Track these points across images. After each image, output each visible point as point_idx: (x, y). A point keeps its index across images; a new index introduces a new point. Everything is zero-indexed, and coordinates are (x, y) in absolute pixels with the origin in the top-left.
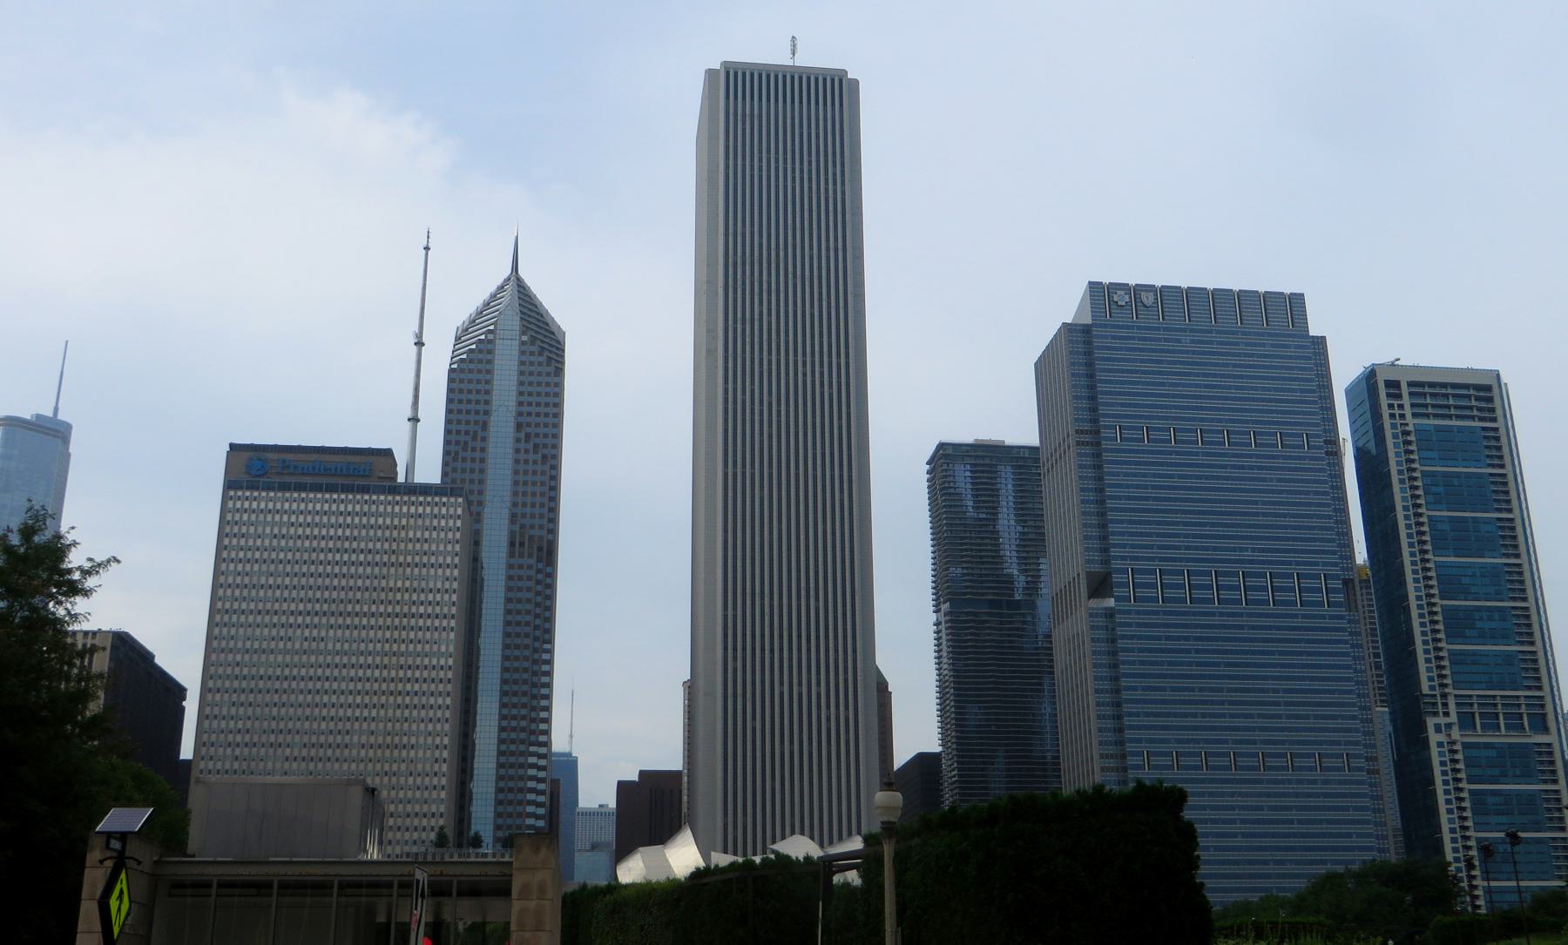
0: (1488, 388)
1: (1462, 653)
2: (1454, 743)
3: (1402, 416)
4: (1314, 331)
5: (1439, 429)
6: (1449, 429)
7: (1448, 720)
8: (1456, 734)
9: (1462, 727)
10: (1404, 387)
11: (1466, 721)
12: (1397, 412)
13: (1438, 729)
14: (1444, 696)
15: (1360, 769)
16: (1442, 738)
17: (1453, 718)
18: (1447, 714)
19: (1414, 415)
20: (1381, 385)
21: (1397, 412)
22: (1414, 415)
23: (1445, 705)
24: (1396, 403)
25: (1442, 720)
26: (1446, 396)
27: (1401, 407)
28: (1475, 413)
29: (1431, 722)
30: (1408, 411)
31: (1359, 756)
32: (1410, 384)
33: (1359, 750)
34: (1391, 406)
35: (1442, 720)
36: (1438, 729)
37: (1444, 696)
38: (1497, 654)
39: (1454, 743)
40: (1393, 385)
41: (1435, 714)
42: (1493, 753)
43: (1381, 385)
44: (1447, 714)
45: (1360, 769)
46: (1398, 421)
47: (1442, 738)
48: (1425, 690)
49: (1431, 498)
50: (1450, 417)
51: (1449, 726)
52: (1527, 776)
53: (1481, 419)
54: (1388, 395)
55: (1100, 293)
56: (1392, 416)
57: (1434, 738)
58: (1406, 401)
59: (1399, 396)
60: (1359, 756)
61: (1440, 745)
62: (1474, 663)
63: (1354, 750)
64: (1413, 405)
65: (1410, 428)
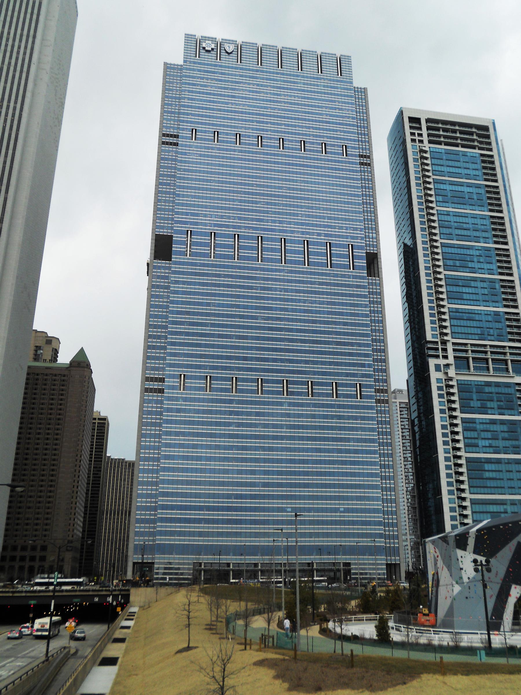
0: (486, 128)
2: (451, 379)
3: (421, 141)
4: (357, 83)
6: (457, 153)
7: (445, 362)
8: (452, 372)
9: (457, 368)
10: (423, 122)
11: (462, 363)
12: (417, 138)
14: (444, 342)
15: (370, 397)
17: (451, 360)
18: (446, 357)
19: (430, 142)
20: (406, 120)
21: (417, 138)
22: (430, 142)
23: (445, 350)
24: (416, 132)
25: (442, 362)
26: (454, 131)
27: (420, 135)
29: (432, 362)
30: (425, 138)
31: (370, 386)
32: (428, 121)
33: (370, 381)
34: (412, 134)
35: (442, 362)
36: (438, 368)
37: (444, 342)
39: (451, 379)
40: (415, 121)
41: (437, 357)
43: (406, 120)
44: (446, 357)
45: (370, 397)
46: (417, 144)
47: (440, 375)
48: (429, 338)
49: (440, 198)
50: (457, 145)
51: (447, 366)
53: (480, 149)
54: (411, 127)
56: (413, 140)
57: (434, 376)
58: (424, 132)
59: (420, 129)
60: (370, 386)
61: (438, 380)
63: (365, 381)
64: (429, 135)
65: (427, 149)
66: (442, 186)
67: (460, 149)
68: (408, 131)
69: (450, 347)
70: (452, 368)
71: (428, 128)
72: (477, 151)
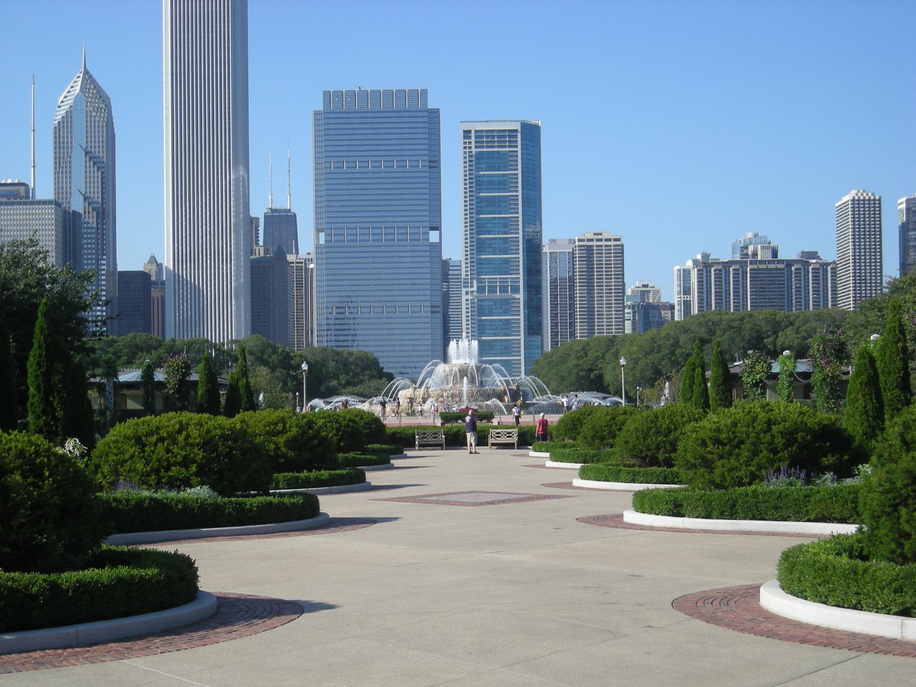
3: (470, 148)
5: (488, 152)
10: (473, 132)
11: (481, 289)
12: (467, 145)
13: (467, 293)
16: (469, 297)
17: (475, 289)
18: (472, 287)
19: (476, 147)
21: (467, 145)
22: (476, 147)
23: (472, 283)
25: (470, 289)
29: (464, 290)
30: (473, 145)
32: (476, 131)
35: (470, 289)
38: (500, 259)
42: (491, 303)
44: (472, 287)
47: (469, 297)
51: (472, 292)
52: (506, 312)
55: (327, 96)
57: (464, 297)
58: (473, 140)
61: (467, 300)
62: (491, 264)
67: (496, 149)
71: (476, 137)
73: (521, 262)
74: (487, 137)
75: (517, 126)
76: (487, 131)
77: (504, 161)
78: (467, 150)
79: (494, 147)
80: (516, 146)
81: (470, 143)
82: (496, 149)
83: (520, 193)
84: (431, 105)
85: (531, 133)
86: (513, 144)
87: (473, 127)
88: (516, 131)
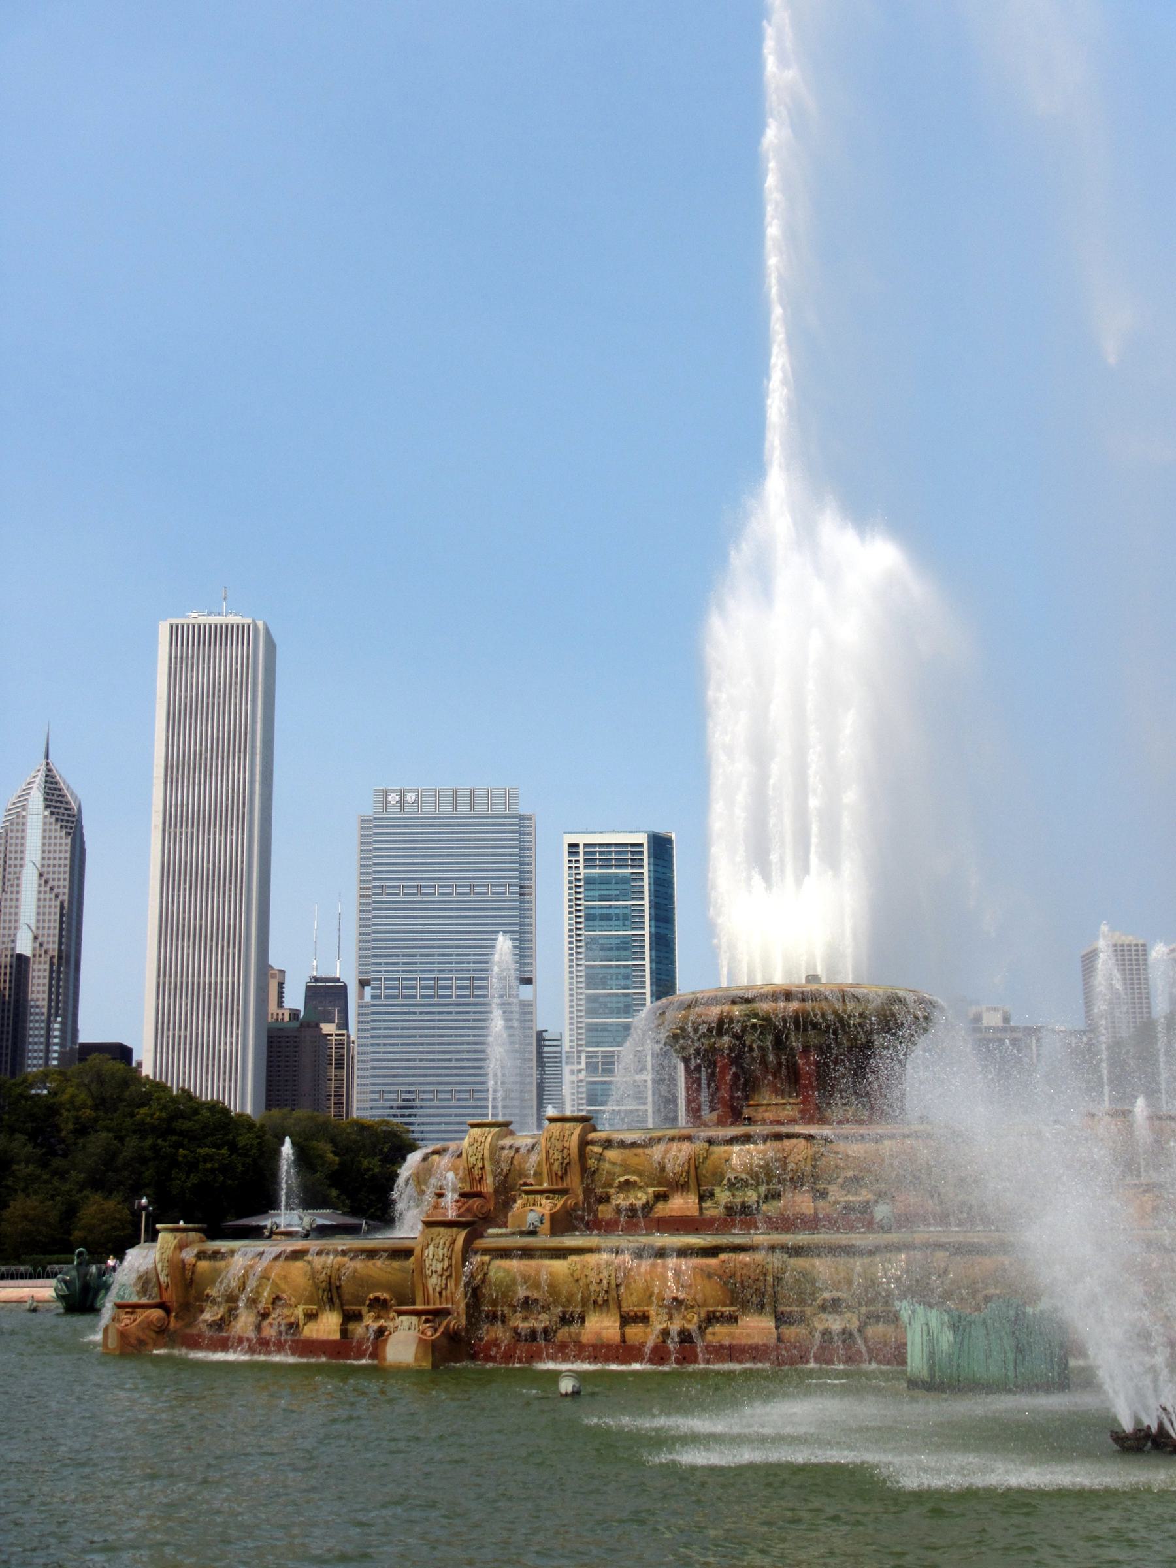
1: (596, 1024)
10: (581, 850)
13: (572, 1072)
16: (574, 1078)
17: (583, 1066)
19: (586, 867)
21: (574, 865)
22: (586, 867)
23: (579, 1057)
25: (576, 1067)
28: (629, 863)
30: (581, 864)
32: (585, 845)
35: (576, 1067)
38: (618, 1024)
44: (579, 1063)
47: (574, 1078)
51: (580, 1071)
53: (633, 867)
58: (581, 857)
59: (577, 854)
62: (605, 1030)
66: (592, 911)
67: (613, 870)
68: (566, 858)
69: (583, 1056)
70: (584, 1073)
71: (586, 853)
72: (630, 870)
73: (646, 881)
74: (601, 853)
75: (642, 838)
76: (601, 845)
77: (628, 886)
78: (574, 871)
79: (610, 867)
80: (642, 867)
81: (577, 861)
82: (613, 870)
83: (647, 932)
84: (523, 810)
85: (661, 847)
86: (637, 862)
87: (582, 839)
88: (641, 845)
